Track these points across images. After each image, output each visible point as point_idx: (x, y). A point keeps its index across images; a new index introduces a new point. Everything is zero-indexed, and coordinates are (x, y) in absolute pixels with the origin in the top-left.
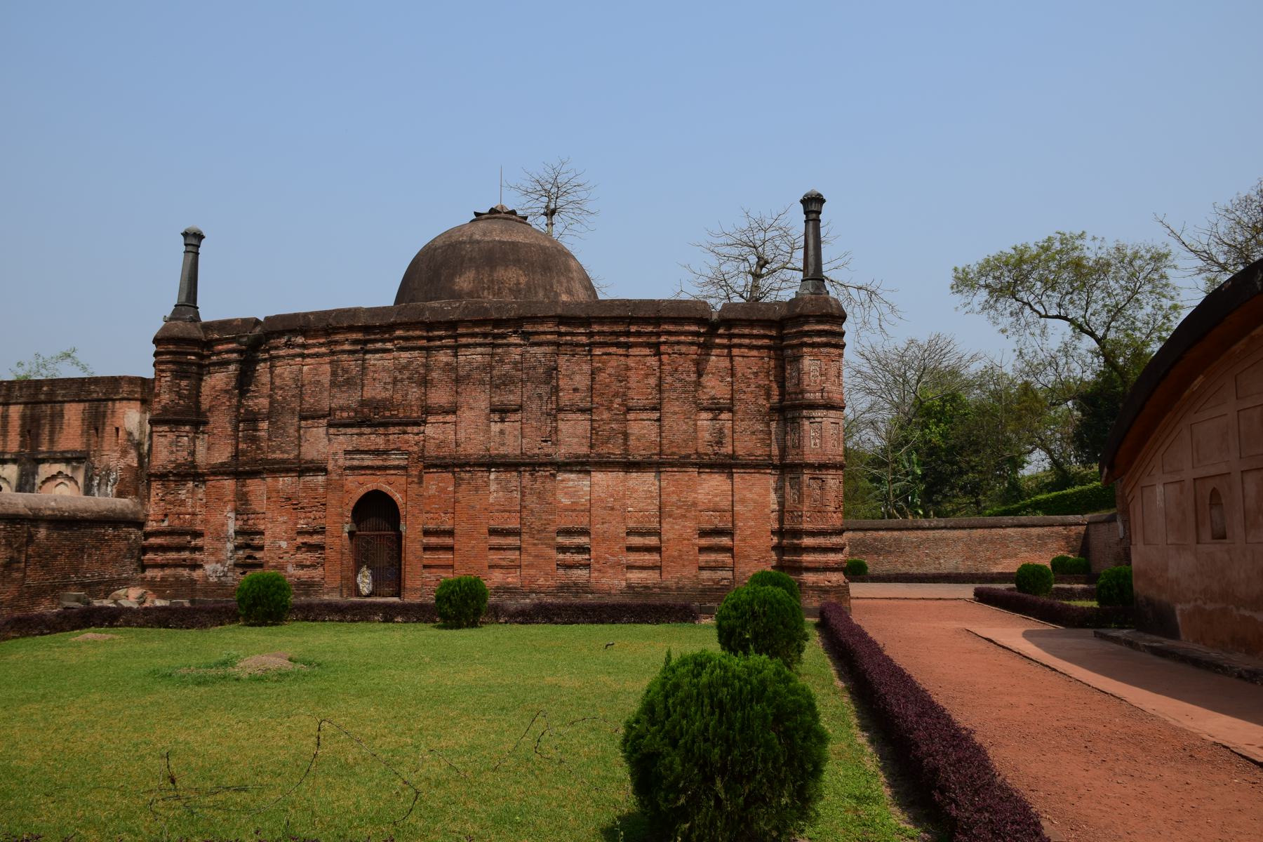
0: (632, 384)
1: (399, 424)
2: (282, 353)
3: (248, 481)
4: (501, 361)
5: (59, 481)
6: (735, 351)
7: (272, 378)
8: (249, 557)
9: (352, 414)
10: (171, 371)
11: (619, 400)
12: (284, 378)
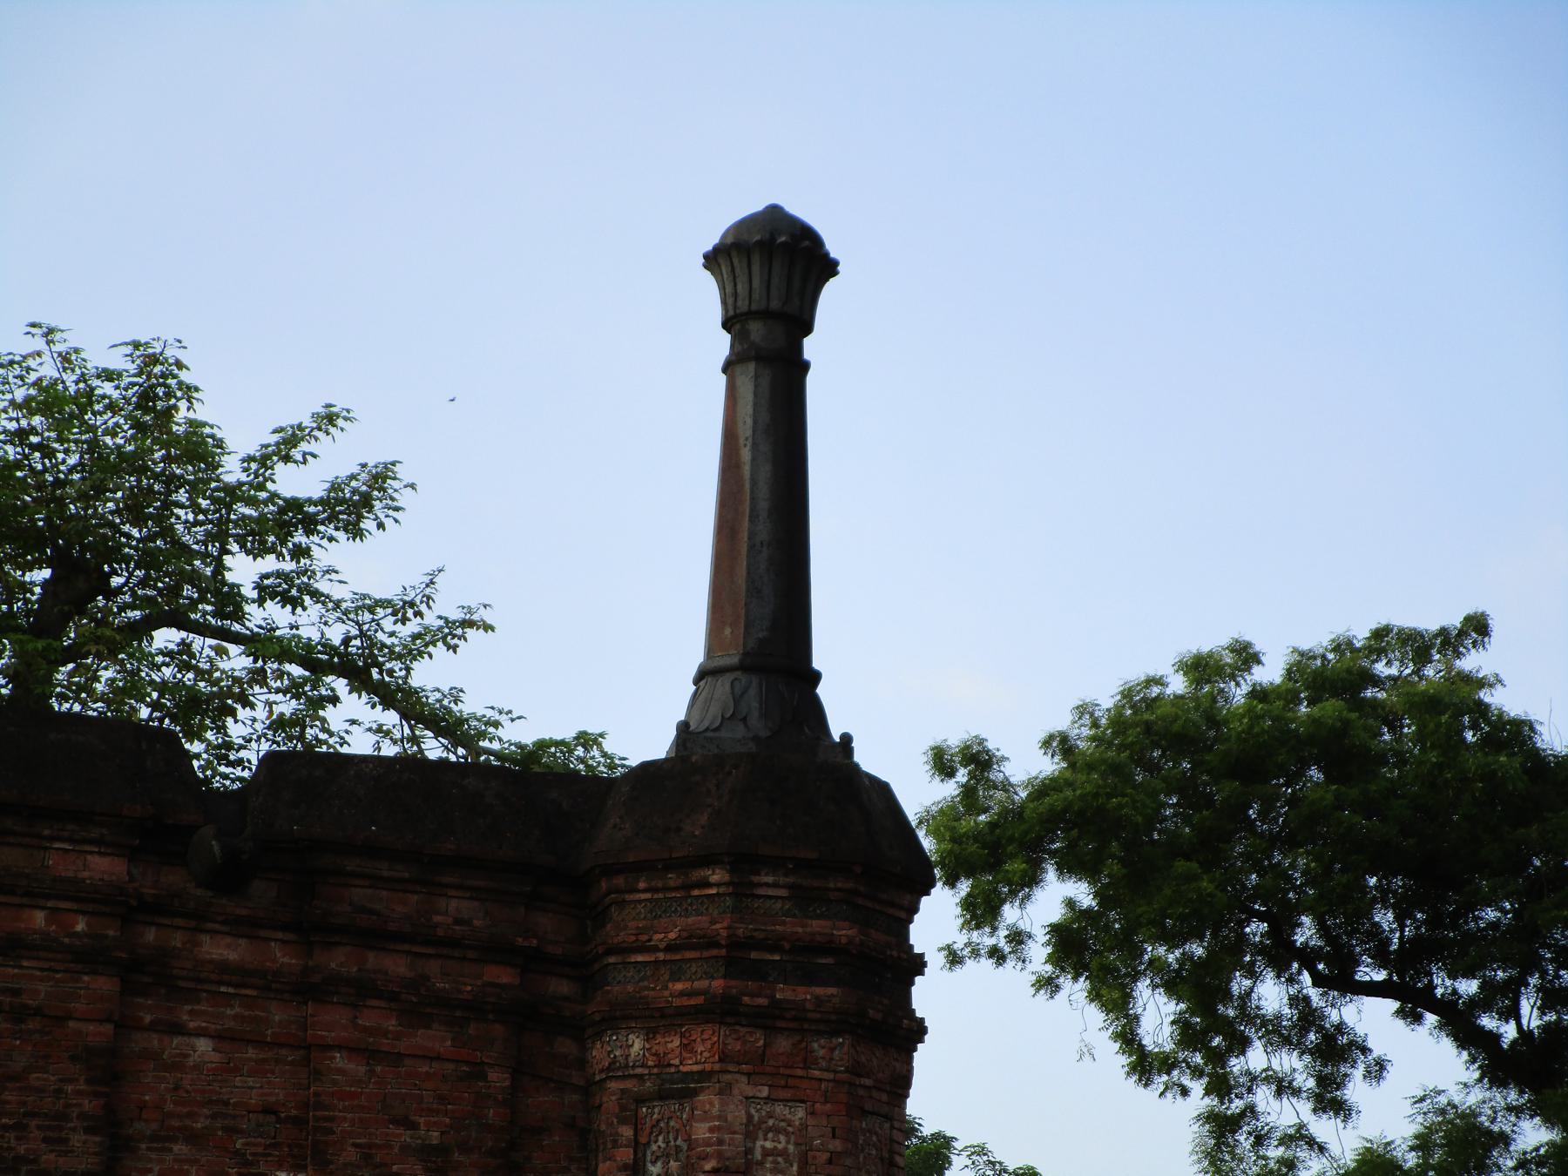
6: (333, 1021)
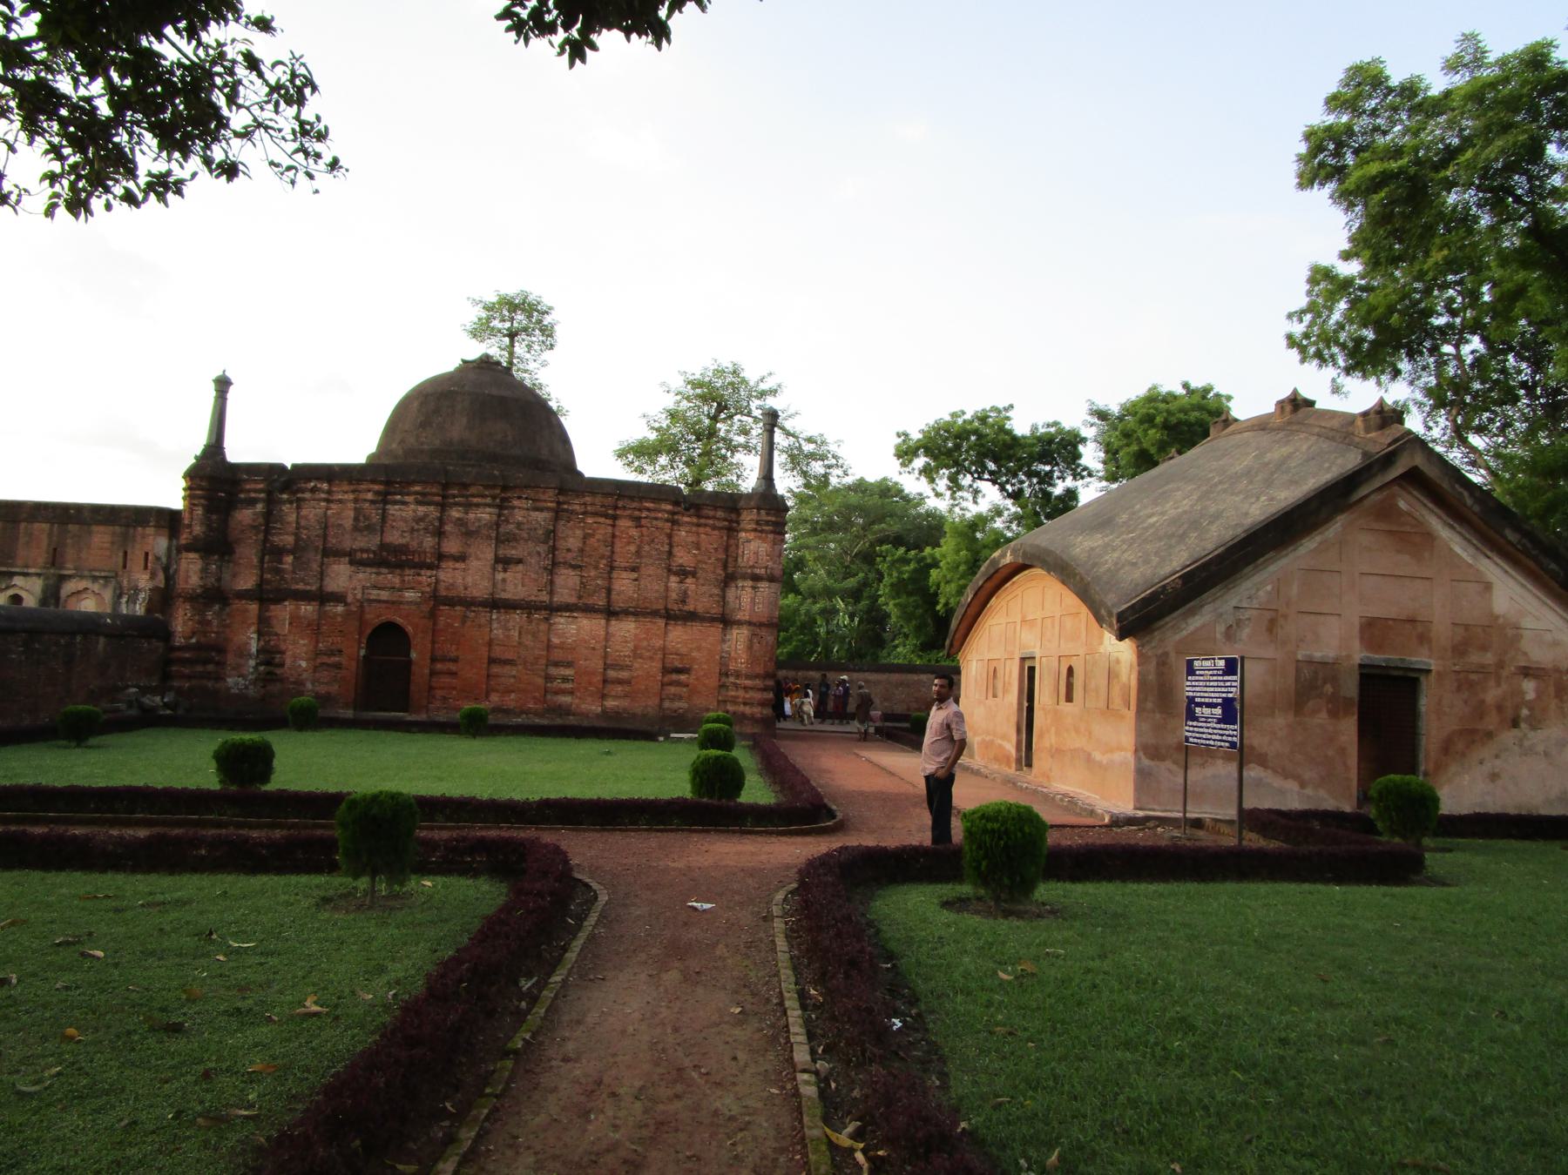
0: (617, 549)
1: (414, 567)
3: (272, 607)
4: (507, 521)
6: (701, 530)
7: (297, 517)
8: (269, 673)
9: (371, 556)
10: (202, 505)
11: (604, 561)
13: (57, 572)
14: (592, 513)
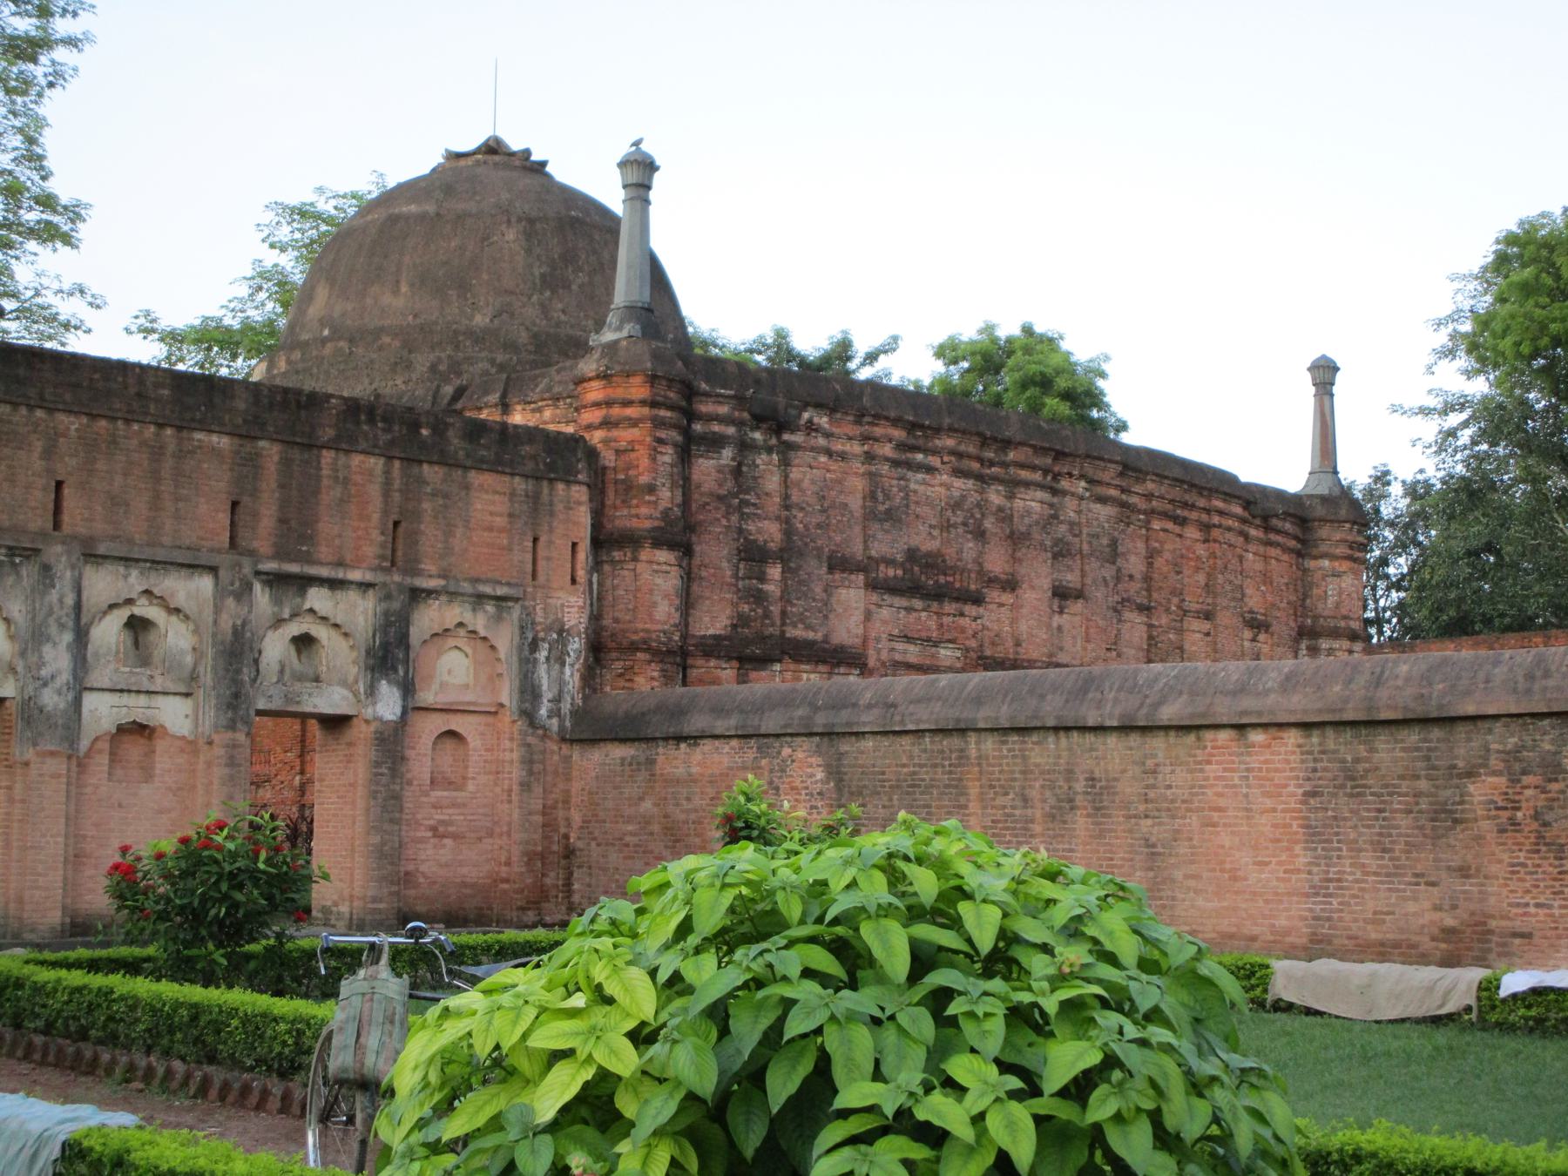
1: (957, 599)
2: (798, 438)
5: (451, 642)
6: (1274, 552)
9: (900, 572)
10: (675, 445)
11: (1175, 600)
12: (802, 491)
13: (409, 581)
14: (1159, 513)
